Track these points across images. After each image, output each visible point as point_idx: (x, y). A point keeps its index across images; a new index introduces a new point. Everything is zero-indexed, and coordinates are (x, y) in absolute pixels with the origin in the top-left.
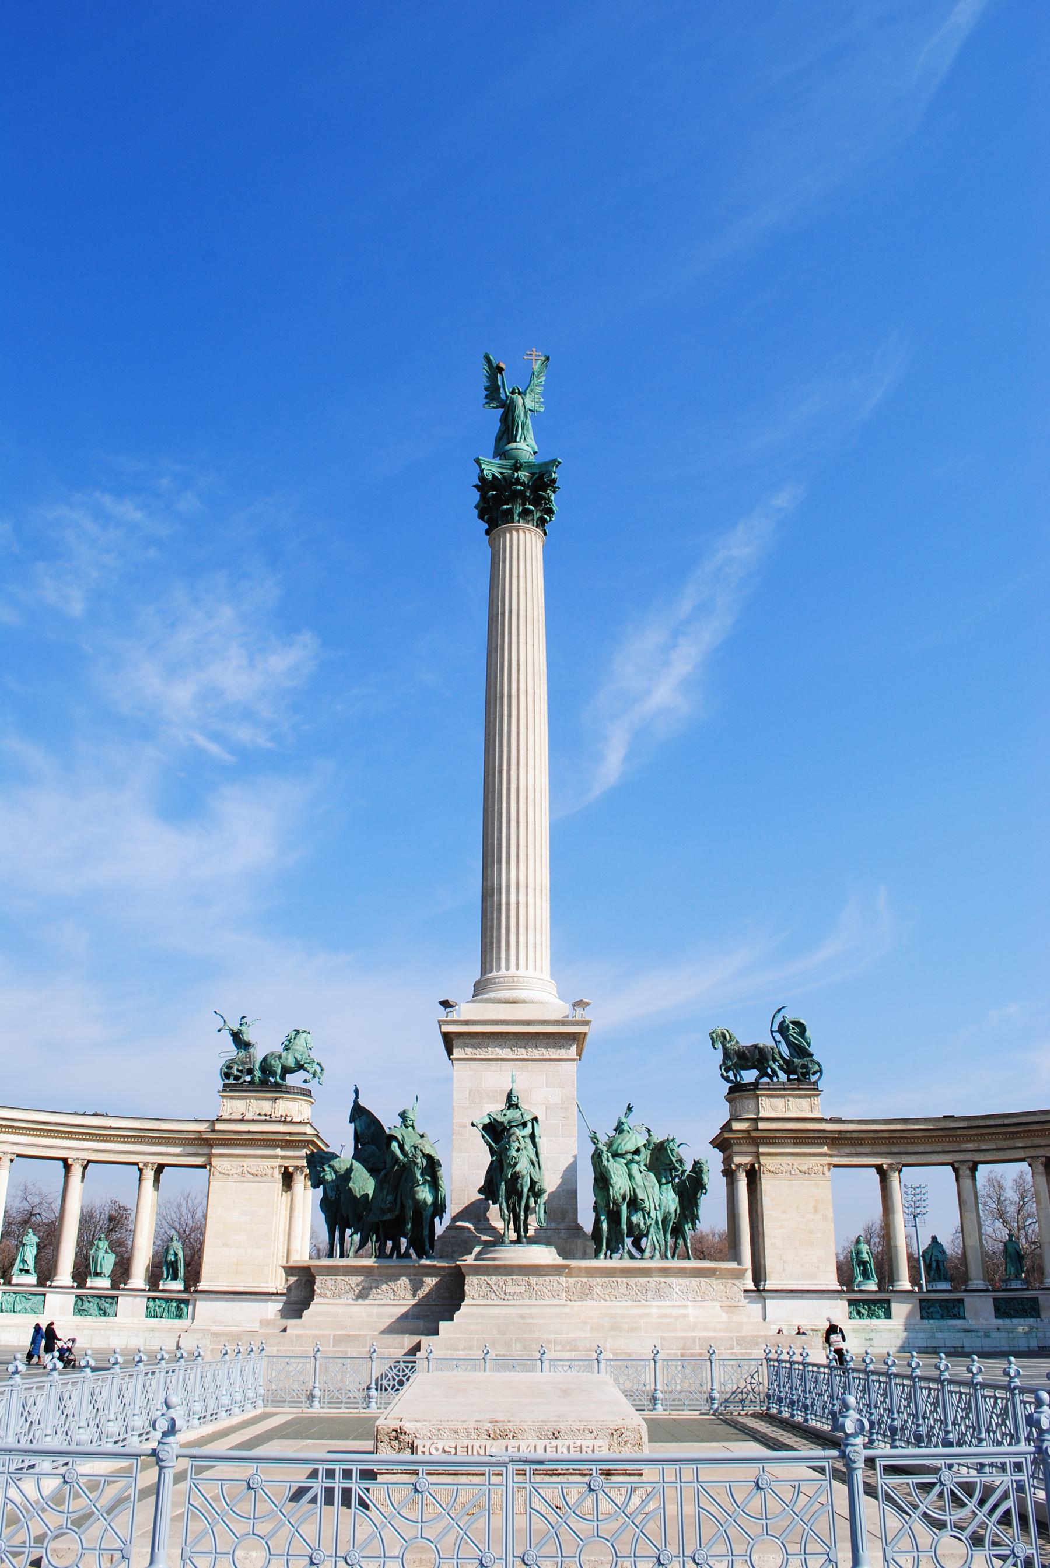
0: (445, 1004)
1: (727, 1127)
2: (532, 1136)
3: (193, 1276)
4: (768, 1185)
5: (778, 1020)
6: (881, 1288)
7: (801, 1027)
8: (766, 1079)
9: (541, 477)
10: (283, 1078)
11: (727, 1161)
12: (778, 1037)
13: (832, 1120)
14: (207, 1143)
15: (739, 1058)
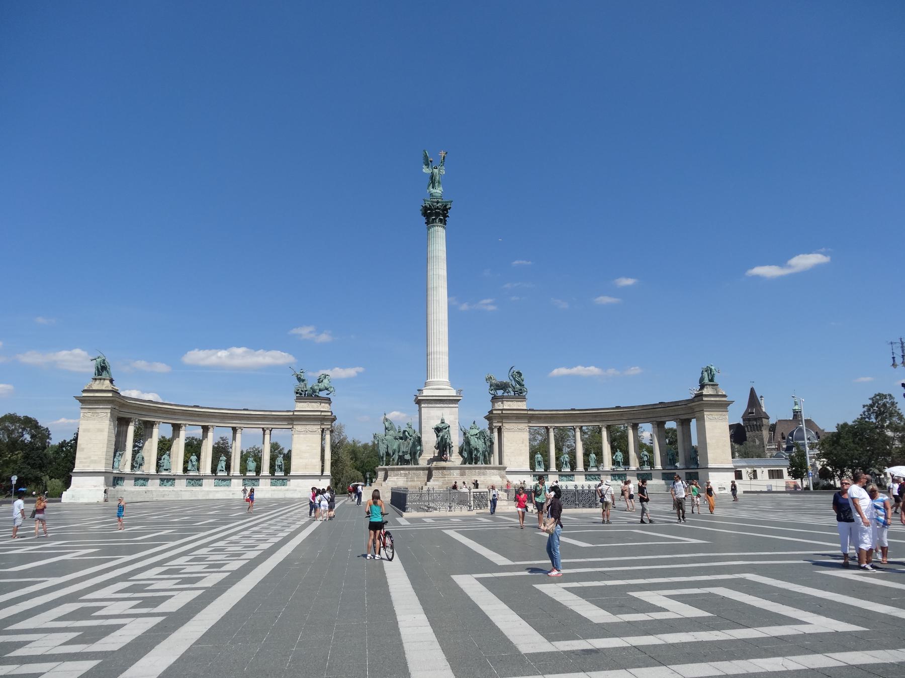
1: (491, 412)
3: (287, 470)
4: (506, 435)
6: (546, 470)
7: (519, 374)
8: (506, 394)
11: (491, 424)
13: (530, 410)
14: (293, 420)
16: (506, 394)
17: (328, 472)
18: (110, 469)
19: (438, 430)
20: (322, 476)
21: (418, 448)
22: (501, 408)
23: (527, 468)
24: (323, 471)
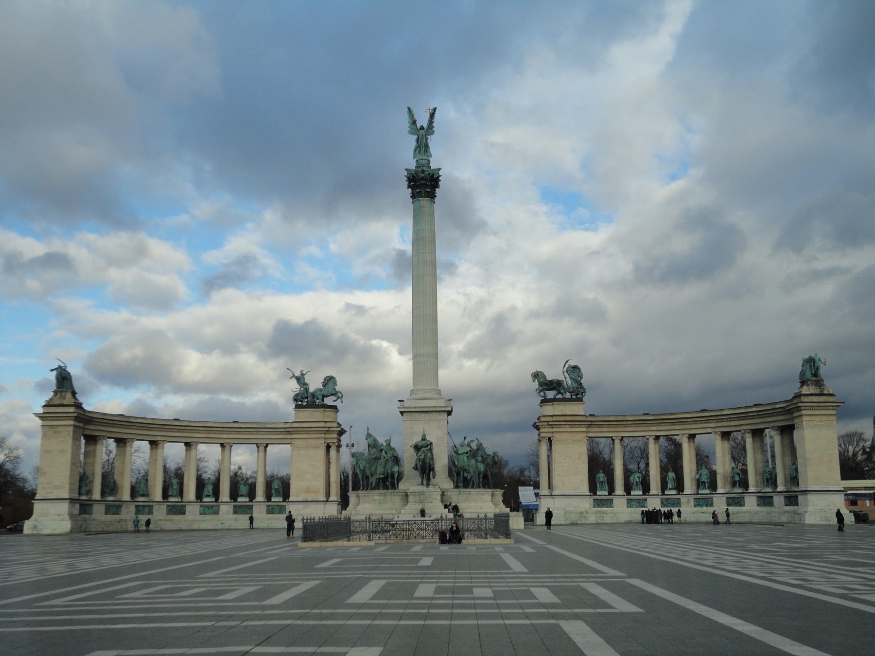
0: (400, 401)
2: (430, 450)
3: (286, 496)
5: (567, 366)
8: (559, 396)
9: (433, 175)
10: (323, 400)
11: (539, 435)
12: (566, 374)
15: (547, 385)
16: (559, 396)
17: (335, 496)
18: (76, 496)
19: (417, 448)
20: (327, 501)
21: (396, 469)
23: (585, 490)
24: (328, 494)
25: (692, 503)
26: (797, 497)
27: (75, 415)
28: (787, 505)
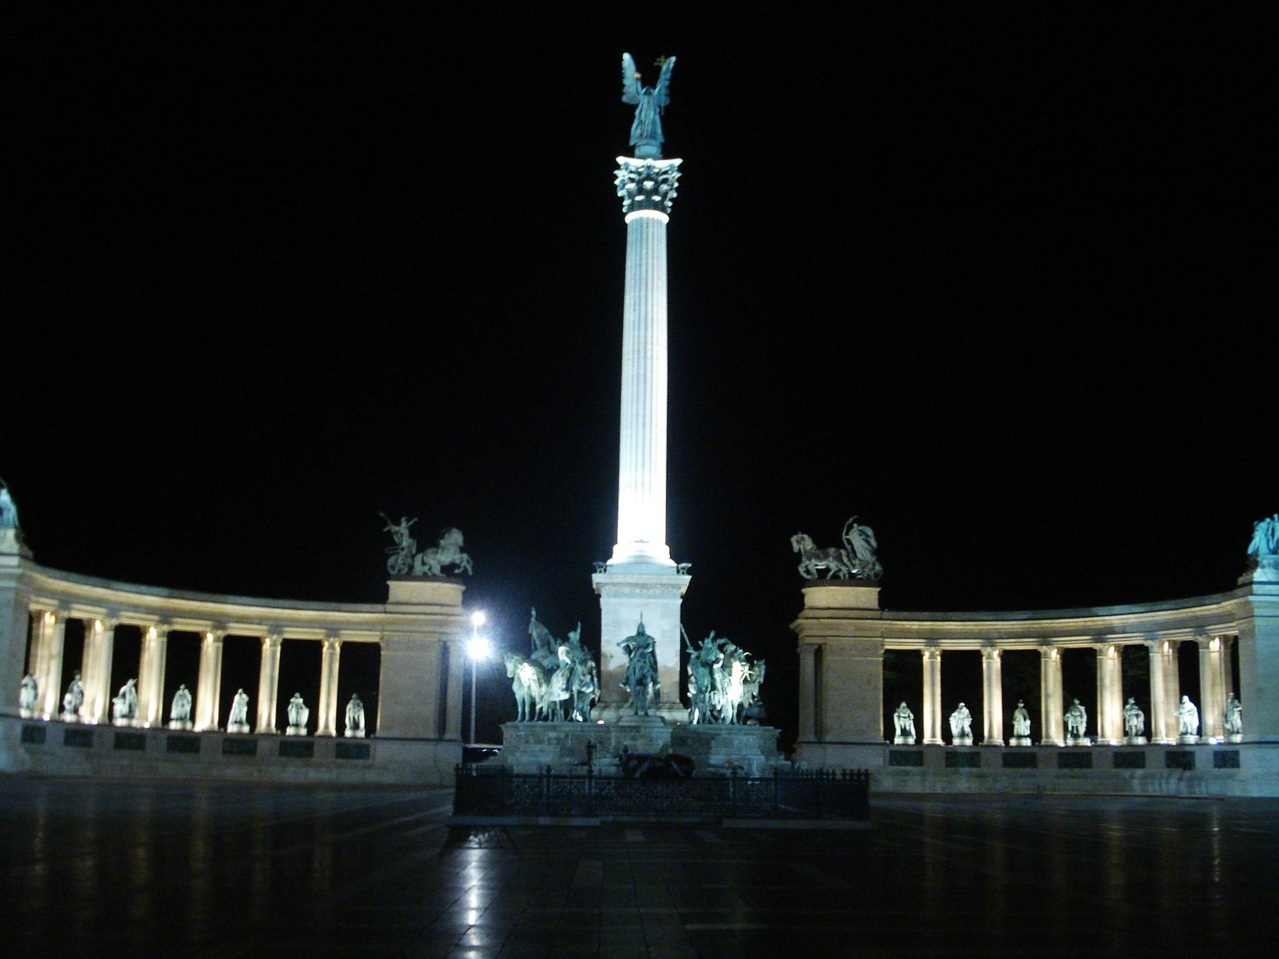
2: (653, 653)
22: (823, 604)
24: (442, 726)
25: (1055, 761)
26: (1237, 753)
27: (19, 571)
28: (1216, 766)
